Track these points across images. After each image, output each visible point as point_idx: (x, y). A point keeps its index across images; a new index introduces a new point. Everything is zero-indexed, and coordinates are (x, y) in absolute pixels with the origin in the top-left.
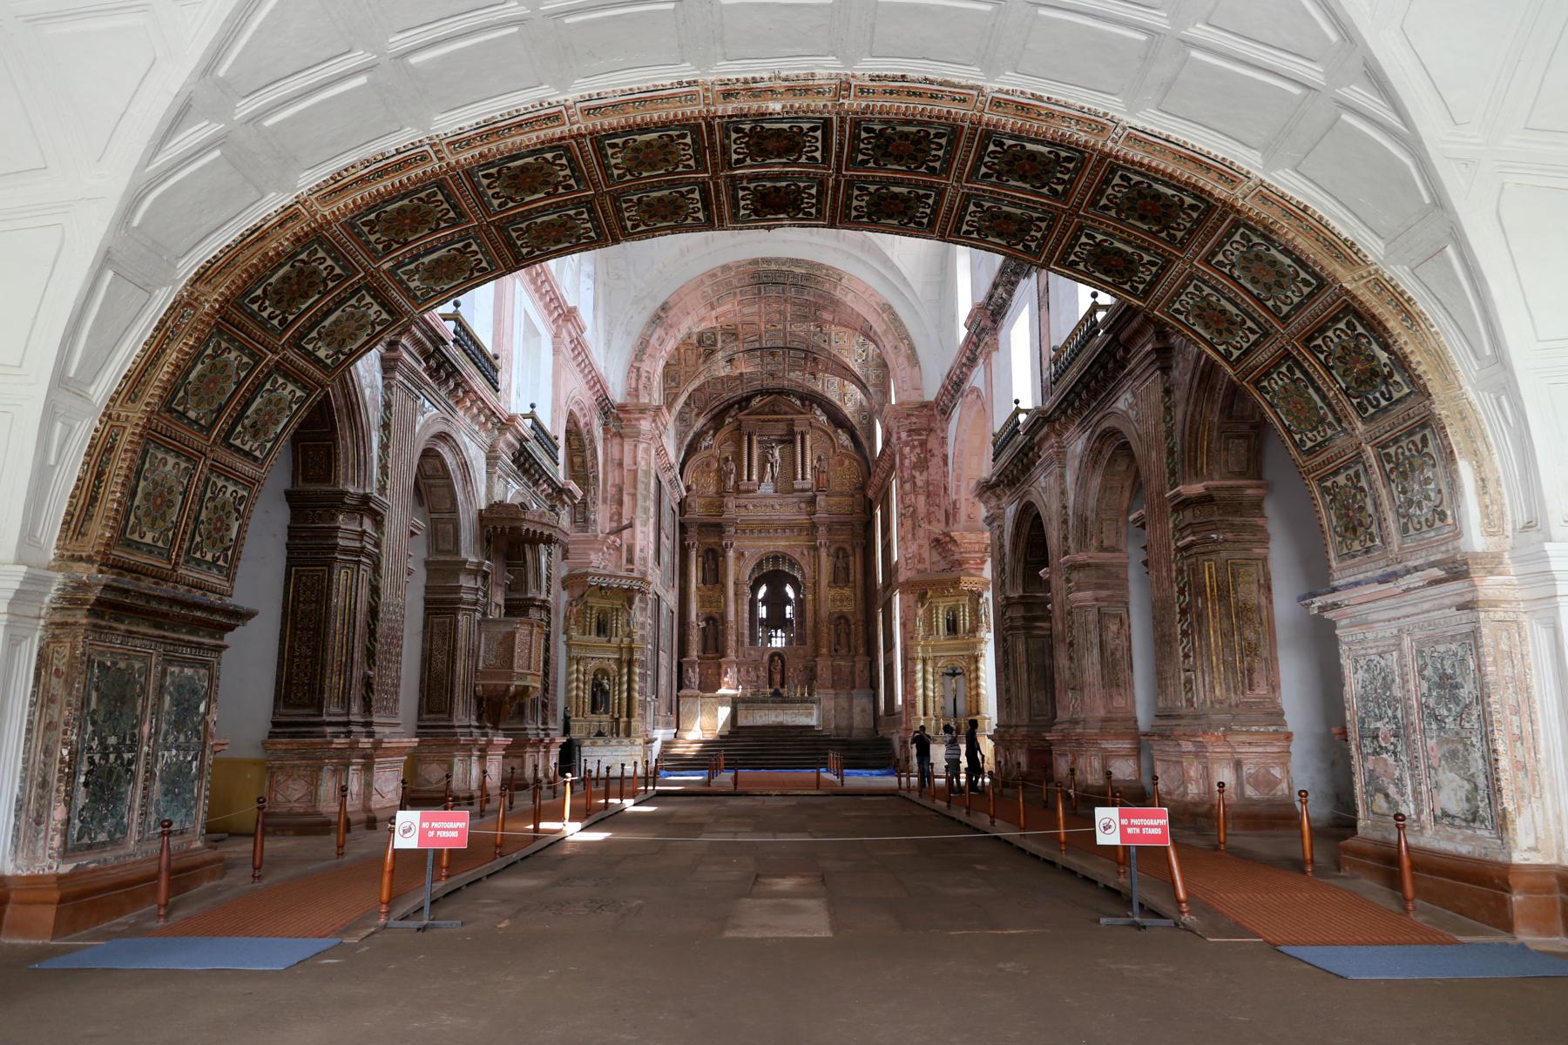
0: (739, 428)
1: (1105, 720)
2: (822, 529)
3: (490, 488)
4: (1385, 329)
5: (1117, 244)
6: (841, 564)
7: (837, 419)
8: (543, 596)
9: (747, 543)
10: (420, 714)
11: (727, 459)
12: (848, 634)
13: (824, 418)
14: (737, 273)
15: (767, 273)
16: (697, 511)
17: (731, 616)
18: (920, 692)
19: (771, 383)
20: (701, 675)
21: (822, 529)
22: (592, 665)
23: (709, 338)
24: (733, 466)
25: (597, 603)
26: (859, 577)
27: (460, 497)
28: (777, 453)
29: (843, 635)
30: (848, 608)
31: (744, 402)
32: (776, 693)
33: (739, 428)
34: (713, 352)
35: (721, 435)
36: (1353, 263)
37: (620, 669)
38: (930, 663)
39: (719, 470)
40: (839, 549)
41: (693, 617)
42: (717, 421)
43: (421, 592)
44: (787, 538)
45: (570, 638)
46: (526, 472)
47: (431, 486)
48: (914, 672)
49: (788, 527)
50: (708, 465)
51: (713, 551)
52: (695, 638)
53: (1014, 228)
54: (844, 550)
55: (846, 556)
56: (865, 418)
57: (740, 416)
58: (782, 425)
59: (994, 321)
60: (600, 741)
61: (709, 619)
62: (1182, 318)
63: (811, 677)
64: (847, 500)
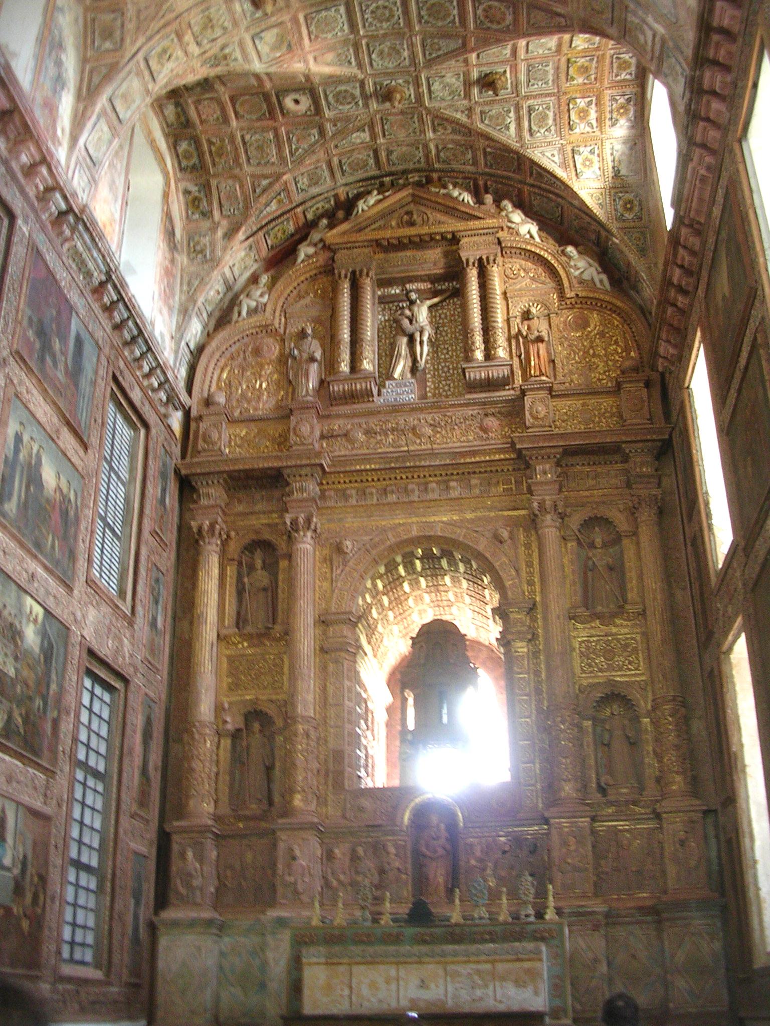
2: (544, 472)
6: (601, 559)
9: (351, 522)
11: (303, 334)
12: (633, 743)
13: (528, 228)
17: (307, 701)
19: (398, 143)
21: (544, 472)
26: (654, 583)
28: (423, 314)
30: (631, 673)
32: (420, 914)
33: (329, 270)
39: (283, 359)
40: (590, 523)
41: (205, 708)
42: (280, 258)
50: (257, 352)
56: (628, 206)
57: (333, 236)
61: (254, 715)
64: (607, 403)
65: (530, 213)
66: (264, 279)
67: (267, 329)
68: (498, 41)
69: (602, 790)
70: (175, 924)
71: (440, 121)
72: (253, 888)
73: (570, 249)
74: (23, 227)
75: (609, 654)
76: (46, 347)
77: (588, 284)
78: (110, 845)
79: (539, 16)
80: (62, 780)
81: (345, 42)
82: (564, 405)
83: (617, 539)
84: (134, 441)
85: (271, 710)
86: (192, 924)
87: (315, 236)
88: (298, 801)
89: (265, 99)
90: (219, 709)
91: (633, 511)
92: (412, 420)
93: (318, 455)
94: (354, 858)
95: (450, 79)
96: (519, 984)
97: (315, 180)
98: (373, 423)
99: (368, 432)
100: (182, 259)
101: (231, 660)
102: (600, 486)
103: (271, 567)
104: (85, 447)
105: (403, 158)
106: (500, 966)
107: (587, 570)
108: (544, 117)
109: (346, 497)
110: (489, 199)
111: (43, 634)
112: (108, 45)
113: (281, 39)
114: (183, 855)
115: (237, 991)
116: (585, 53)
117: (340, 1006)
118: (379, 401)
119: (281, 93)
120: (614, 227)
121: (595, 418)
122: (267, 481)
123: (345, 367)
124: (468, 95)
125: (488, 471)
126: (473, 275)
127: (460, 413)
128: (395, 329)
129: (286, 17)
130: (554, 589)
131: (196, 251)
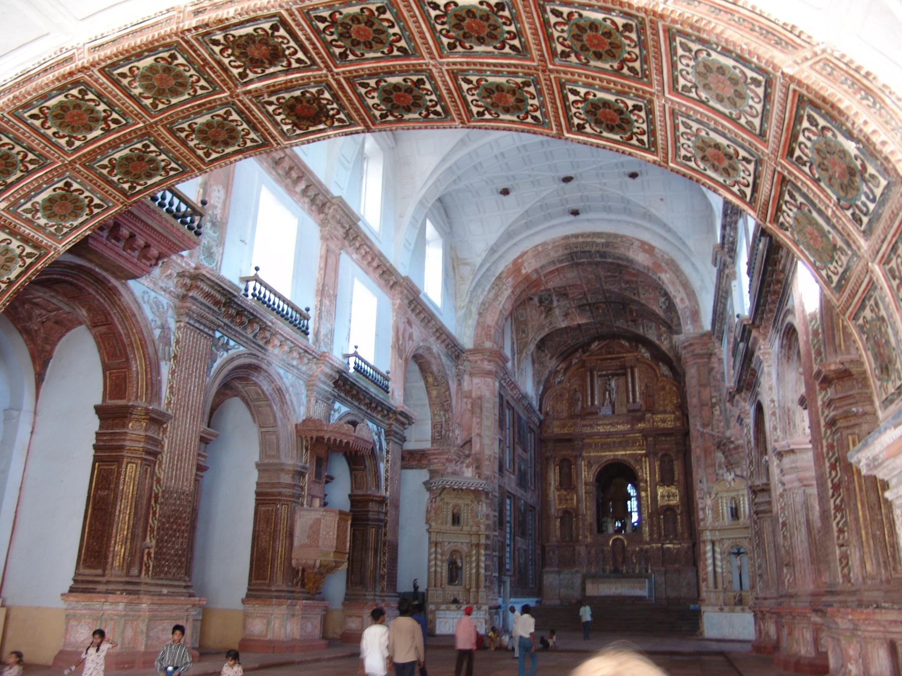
0: (583, 366)
1: (813, 595)
3: (308, 409)
4: (840, 112)
5: (600, 95)
8: (383, 493)
10: (250, 581)
11: (575, 391)
13: (647, 355)
14: (553, 247)
15: (576, 245)
18: (710, 568)
22: (447, 548)
23: (547, 299)
24: (579, 395)
25: (451, 501)
26: (682, 477)
27: (279, 415)
30: (674, 501)
31: (585, 347)
33: (583, 366)
34: (551, 309)
36: (796, 47)
37: (470, 552)
38: (717, 544)
40: (664, 455)
43: (254, 488)
45: (430, 526)
46: (356, 397)
47: (259, 406)
48: (705, 553)
50: (561, 395)
51: (567, 460)
53: (512, 100)
57: (584, 357)
59: (731, 257)
60: (453, 607)
62: (692, 164)
65: (648, 350)
71: (617, 327)
73: (660, 364)
75: (669, 496)
77: (666, 376)
83: (672, 461)
87: (578, 355)
96: (641, 589)
100: (536, 365)
108: (651, 328)
110: (634, 344)
112: (524, 335)
117: (595, 594)
122: (567, 440)
126: (629, 370)
128: (605, 389)
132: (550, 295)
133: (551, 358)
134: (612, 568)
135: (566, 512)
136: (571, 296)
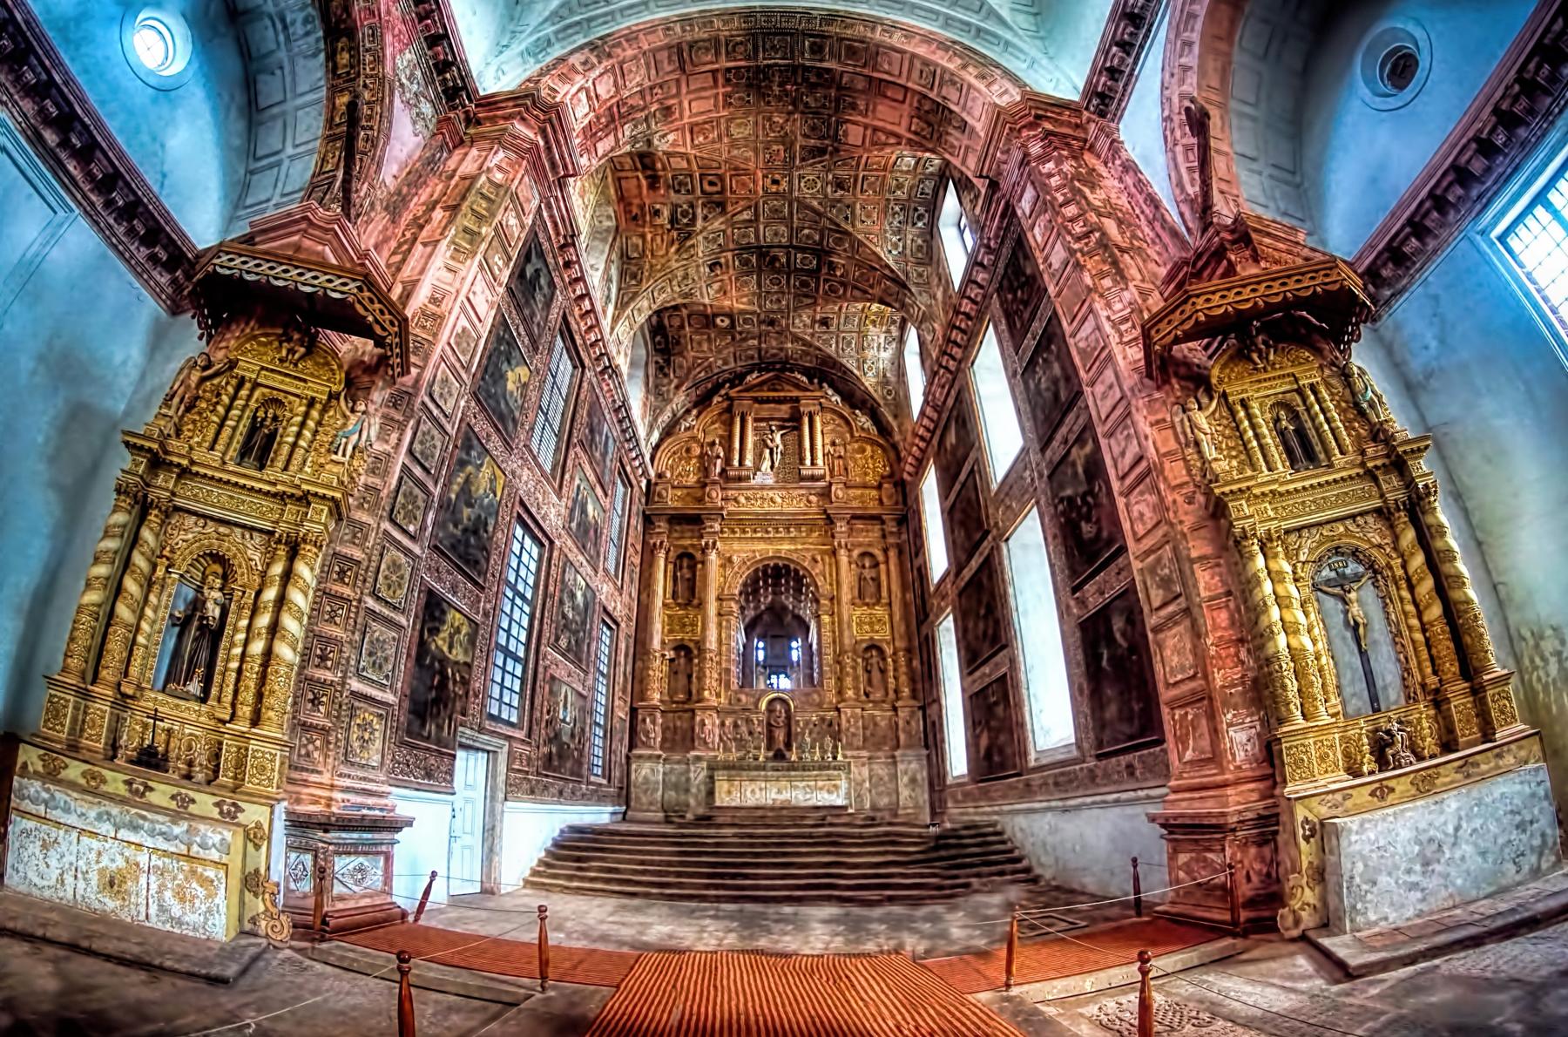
0: (729, 410)
2: (841, 527)
6: (868, 574)
7: (855, 398)
9: (736, 546)
11: (713, 444)
12: (883, 671)
13: (836, 398)
16: (672, 500)
17: (712, 642)
20: (665, 729)
26: (895, 588)
29: (876, 675)
30: (882, 634)
31: (737, 378)
34: (689, 236)
35: (708, 416)
39: (701, 457)
40: (863, 555)
41: (656, 643)
44: (793, 540)
49: (793, 523)
50: (688, 450)
51: (691, 557)
52: (658, 670)
54: (871, 555)
55: (876, 565)
58: (785, 407)
61: (680, 647)
63: (833, 730)
65: (837, 391)
66: (695, 412)
67: (694, 438)
68: (835, 303)
69: (867, 695)
70: (640, 757)
71: (796, 339)
72: (682, 738)
74: (588, 374)
75: (871, 624)
76: (593, 439)
78: (610, 712)
79: (857, 293)
80: (591, 676)
81: (754, 294)
82: (851, 492)
84: (625, 494)
85: (692, 645)
86: (650, 757)
87: (723, 392)
88: (706, 693)
89: (707, 320)
90: (663, 642)
91: (885, 551)
92: (771, 494)
93: (722, 508)
94: (736, 726)
95: (805, 318)
96: (829, 792)
97: (726, 363)
98: (749, 493)
99: (747, 499)
101: (669, 616)
102: (869, 536)
103: (692, 568)
104: (606, 495)
105: (774, 355)
106: (820, 784)
107: (861, 578)
108: (850, 343)
109: (734, 532)
111: (584, 596)
113: (721, 288)
114: (644, 721)
115: (673, 793)
116: (875, 314)
118: (753, 482)
119: (715, 315)
120: (882, 402)
121: (869, 501)
122: (691, 521)
123: (736, 463)
124: (812, 327)
125: (812, 525)
126: (806, 420)
127: (795, 493)
129: (725, 277)
130: (845, 588)
131: (659, 394)
132: (692, 206)
133: (677, 387)
134: (771, 754)
135: (680, 647)
136: (730, 208)
